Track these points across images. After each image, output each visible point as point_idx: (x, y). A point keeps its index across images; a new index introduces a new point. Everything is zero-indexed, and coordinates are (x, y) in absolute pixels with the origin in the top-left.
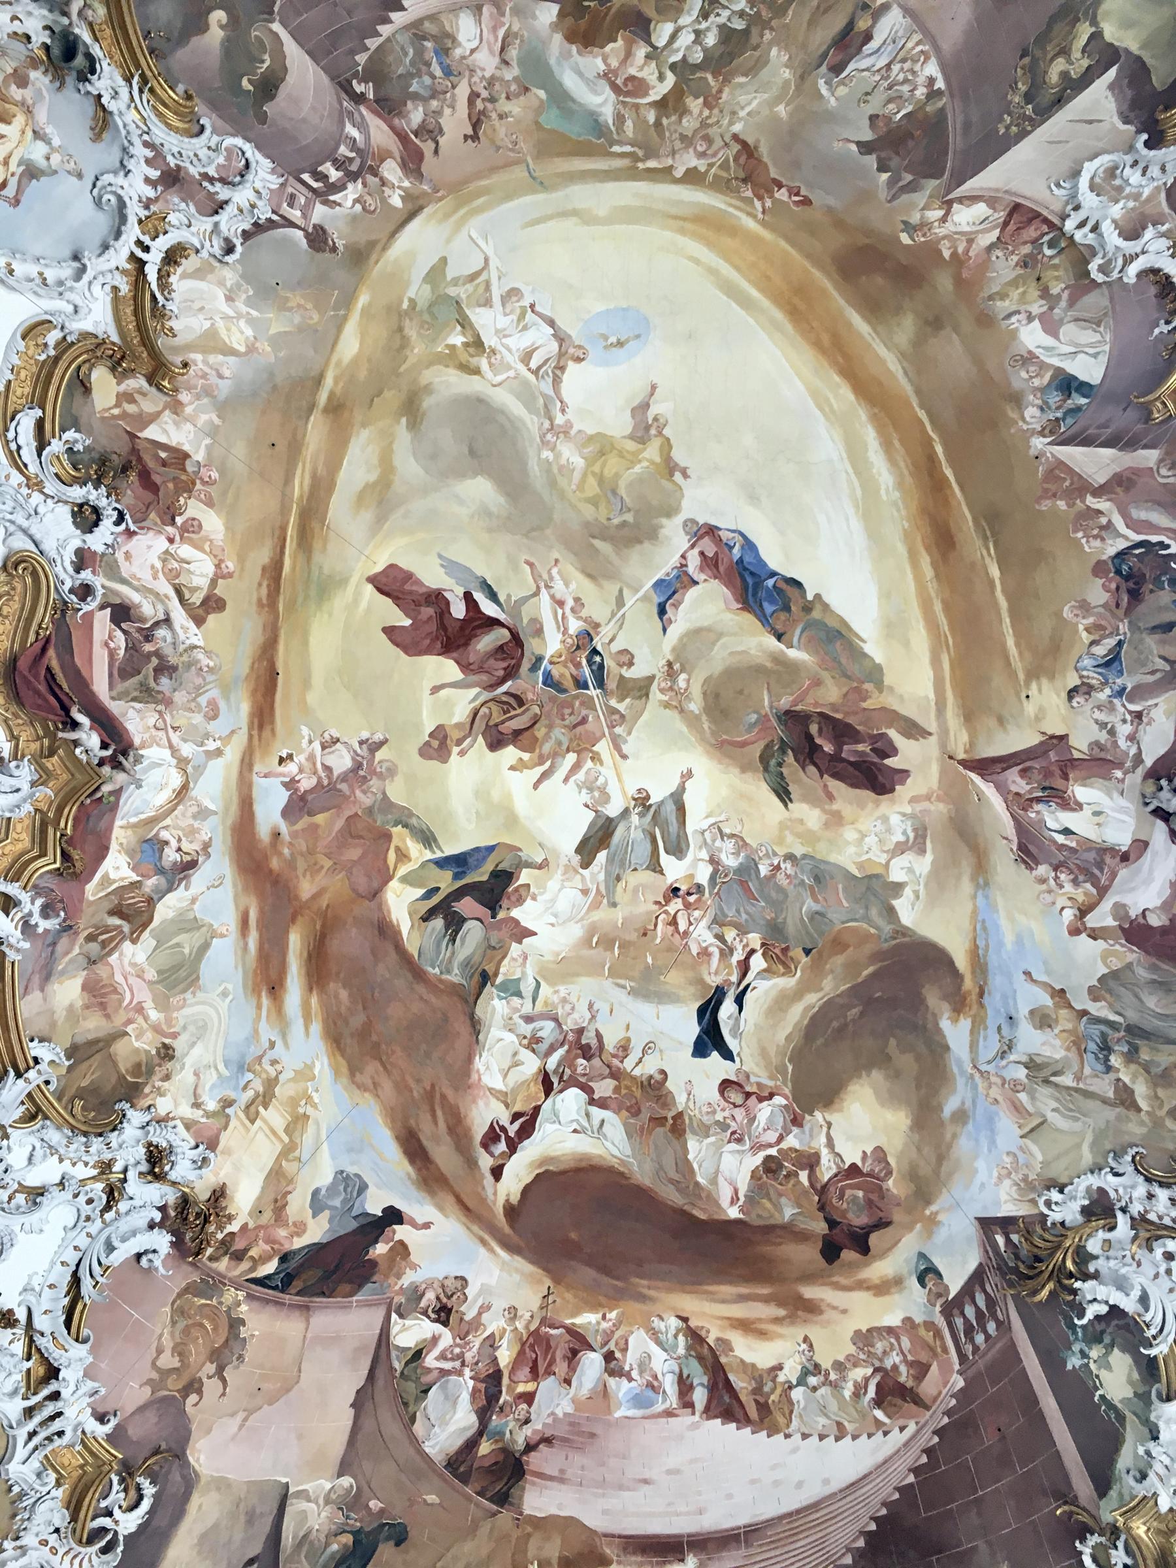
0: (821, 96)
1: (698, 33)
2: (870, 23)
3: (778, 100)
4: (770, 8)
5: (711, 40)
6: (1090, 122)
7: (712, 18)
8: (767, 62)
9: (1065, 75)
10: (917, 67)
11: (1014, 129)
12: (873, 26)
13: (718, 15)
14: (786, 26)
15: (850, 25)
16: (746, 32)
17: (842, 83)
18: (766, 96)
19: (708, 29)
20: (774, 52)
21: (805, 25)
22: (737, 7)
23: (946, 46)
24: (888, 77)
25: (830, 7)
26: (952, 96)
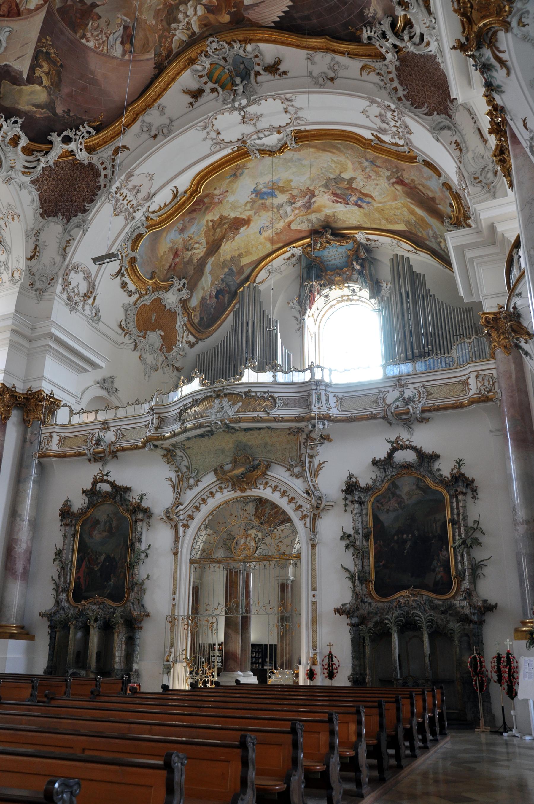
0: (125, 15)
1: (187, 16)
2: (125, 48)
3: (141, 5)
4: (166, 36)
5: (181, 16)
6: (18, 58)
7: (185, 23)
8: (154, 17)
9: (41, 67)
10: (96, 42)
11: (44, 41)
12: (123, 48)
13: (184, 25)
14: (156, 33)
15: (131, 43)
16: (169, 25)
17: (121, 24)
18: (146, 6)
19: (184, 19)
20: (154, 23)
21: (149, 36)
22: (178, 31)
23: (91, 54)
24: (105, 34)
25: (144, 46)
26: (76, 40)
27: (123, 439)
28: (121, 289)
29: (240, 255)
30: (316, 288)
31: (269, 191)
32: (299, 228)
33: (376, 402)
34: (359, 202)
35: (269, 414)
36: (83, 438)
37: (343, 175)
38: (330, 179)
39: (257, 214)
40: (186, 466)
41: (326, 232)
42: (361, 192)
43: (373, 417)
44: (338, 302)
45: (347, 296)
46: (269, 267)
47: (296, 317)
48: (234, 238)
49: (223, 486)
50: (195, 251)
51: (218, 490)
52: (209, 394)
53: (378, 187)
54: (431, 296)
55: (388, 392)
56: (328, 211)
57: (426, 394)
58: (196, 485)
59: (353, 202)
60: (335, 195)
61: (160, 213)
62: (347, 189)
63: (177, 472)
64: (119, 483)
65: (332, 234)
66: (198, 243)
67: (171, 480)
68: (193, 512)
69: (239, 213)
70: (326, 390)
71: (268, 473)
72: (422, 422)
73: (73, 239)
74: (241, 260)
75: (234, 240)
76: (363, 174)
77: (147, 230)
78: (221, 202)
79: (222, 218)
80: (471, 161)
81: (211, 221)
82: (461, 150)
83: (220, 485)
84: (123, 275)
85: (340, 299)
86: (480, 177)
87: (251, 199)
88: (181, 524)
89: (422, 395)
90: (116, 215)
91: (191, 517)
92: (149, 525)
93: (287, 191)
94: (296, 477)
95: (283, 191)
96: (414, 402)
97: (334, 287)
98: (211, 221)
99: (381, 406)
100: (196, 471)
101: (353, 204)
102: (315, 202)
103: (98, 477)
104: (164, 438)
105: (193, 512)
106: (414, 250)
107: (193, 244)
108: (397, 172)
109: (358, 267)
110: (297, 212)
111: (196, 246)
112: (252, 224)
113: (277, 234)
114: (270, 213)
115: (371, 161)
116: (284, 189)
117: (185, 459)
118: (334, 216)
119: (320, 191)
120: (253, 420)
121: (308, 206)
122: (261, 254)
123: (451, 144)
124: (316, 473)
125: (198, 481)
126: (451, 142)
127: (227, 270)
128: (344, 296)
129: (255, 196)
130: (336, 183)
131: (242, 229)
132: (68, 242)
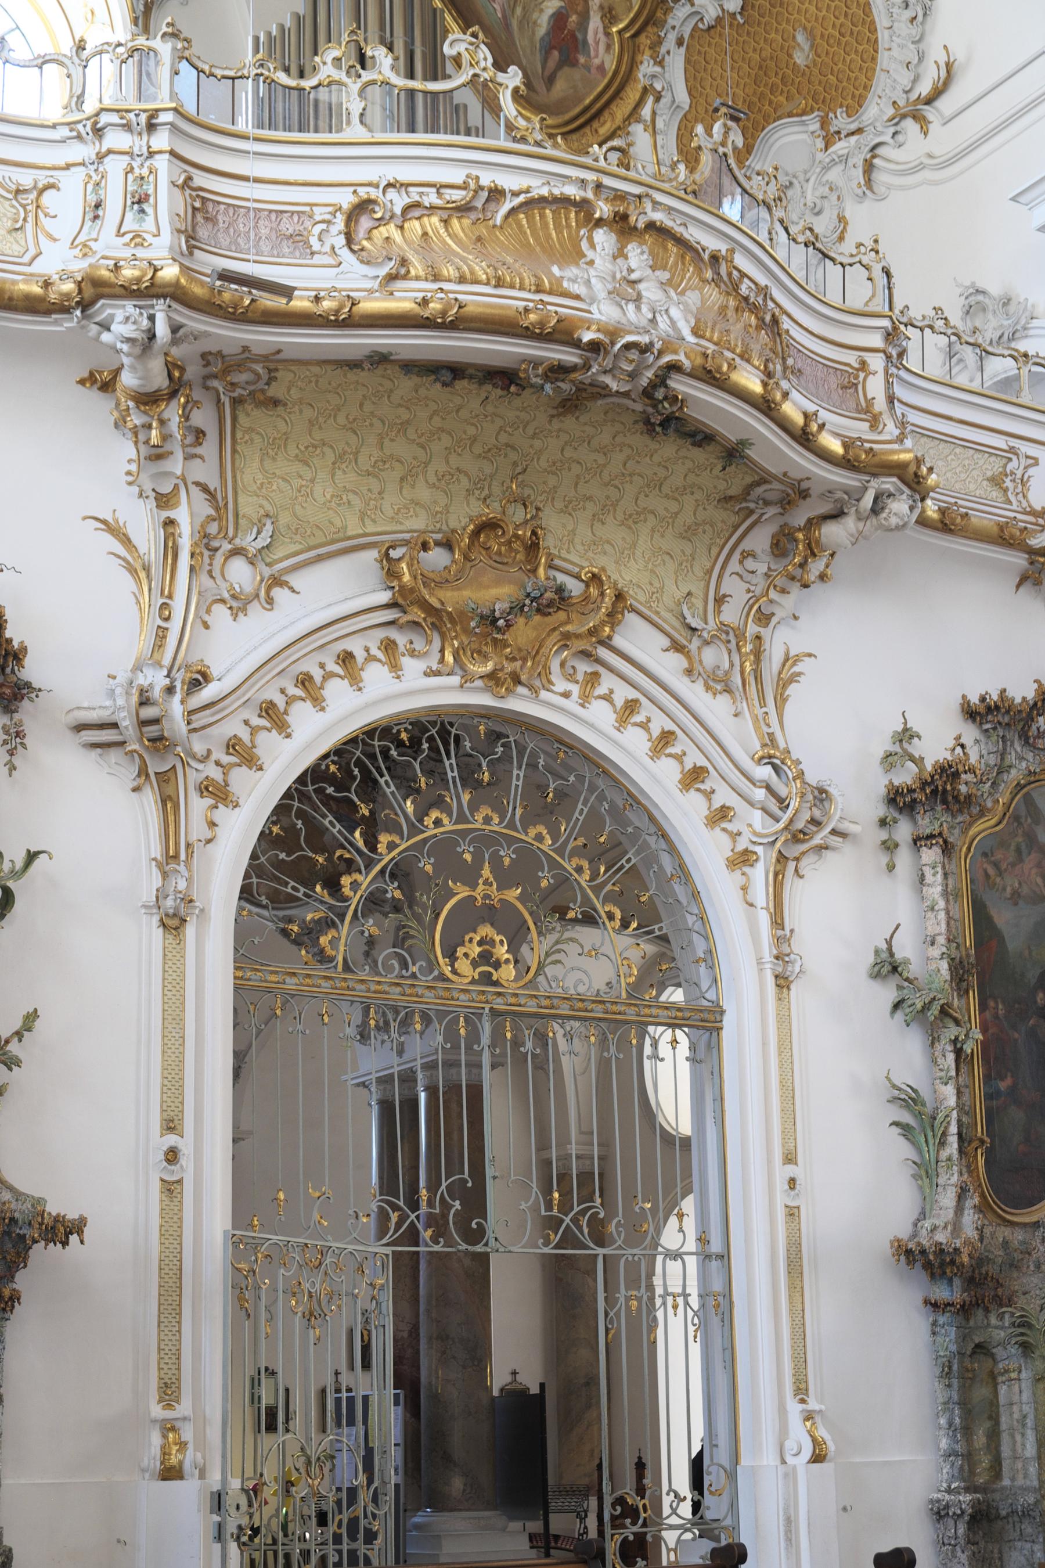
33: (996, 481)
40: (205, 489)
49: (401, 639)
52: (571, 191)
63: (164, 501)
67: (126, 540)
68: (254, 730)
83: (393, 634)
94: (708, 688)
99: (1014, 507)
100: (268, 528)
105: (254, 730)
125: (277, 581)
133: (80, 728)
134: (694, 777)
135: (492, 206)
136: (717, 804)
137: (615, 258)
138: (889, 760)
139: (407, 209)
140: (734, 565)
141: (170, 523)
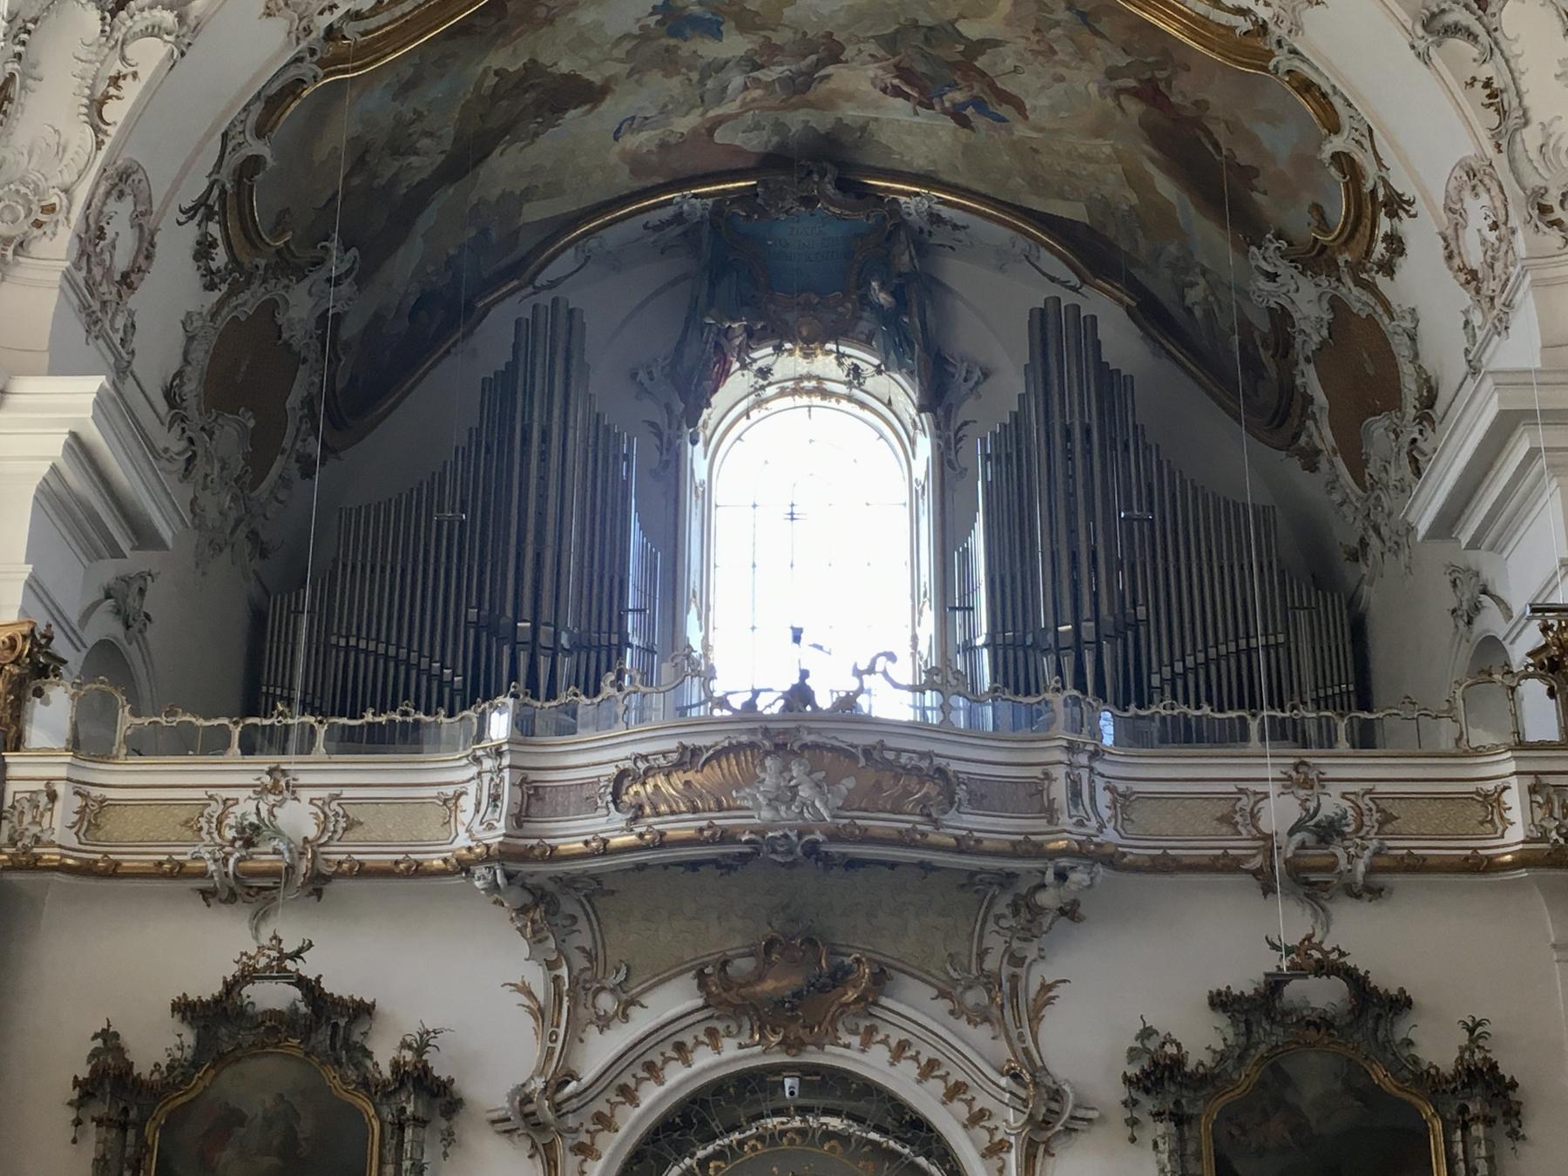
27: (350, 835)
28: (191, 260)
29: (528, 195)
30: (737, 342)
31: (708, 16)
32: (737, 143)
33: (1226, 819)
34: (970, 111)
35: (936, 823)
36: (183, 814)
37: (962, 26)
38: (915, 25)
39: (636, 76)
40: (583, 949)
41: (822, 176)
42: (992, 85)
43: (1226, 865)
44: (783, 393)
45: (819, 379)
46: (593, 243)
47: (652, 424)
48: (537, 135)
50: (413, 159)
51: (702, 1038)
52: (744, 739)
53: (1059, 87)
54: (1147, 447)
55: (1266, 795)
56: (851, 113)
57: (1376, 816)
58: (626, 1017)
59: (947, 104)
60: (903, 72)
61: (372, 23)
62: (955, 66)
63: (551, 965)
64: (328, 986)
65: (843, 185)
66: (430, 135)
67: (530, 994)
69: (586, 63)
70: (1070, 765)
71: (884, 1001)
72: (1358, 896)
73: (135, 75)
74: (526, 207)
75: (533, 142)
76: (1034, 38)
77: (321, 73)
78: (550, 21)
79: (533, 67)
80: (1534, 154)
81: (496, 73)
82: (1502, 113)
84: (208, 217)
85: (790, 384)
86: (1557, 209)
87: (641, 28)
88: (569, 1142)
89: (1366, 819)
90: (269, 15)
91: (605, 1122)
92: (449, 1138)
93: (763, 27)
95: (747, 23)
96: (1342, 835)
97: (788, 346)
98: (496, 73)
99: (1245, 835)
100: (624, 970)
101: (945, 112)
102: (828, 77)
103: (263, 962)
104: (553, 856)
105: (613, 1105)
106: (1075, 281)
107: (415, 137)
108: (1159, 65)
109: (883, 298)
110: (758, 93)
111: (425, 142)
112: (608, 102)
113: (664, 146)
114: (675, 84)
115: (1082, 15)
116: (757, 20)
117: (582, 924)
118: (863, 129)
119: (860, 51)
120: (903, 840)
121: (799, 87)
122: (589, 200)
123: (1472, 84)
124: (1036, 1018)
125: (632, 1002)
126: (1474, 79)
127: (472, 233)
128: (809, 377)
129: (658, 22)
130: (927, 40)
131: (572, 113)
132: (115, 81)
133: (494, 1122)
134: (955, 1091)
135: (696, 759)
136: (976, 1109)
137: (781, 773)
138: (1133, 1054)
139: (646, 772)
140: (991, 926)
141: (557, 979)
